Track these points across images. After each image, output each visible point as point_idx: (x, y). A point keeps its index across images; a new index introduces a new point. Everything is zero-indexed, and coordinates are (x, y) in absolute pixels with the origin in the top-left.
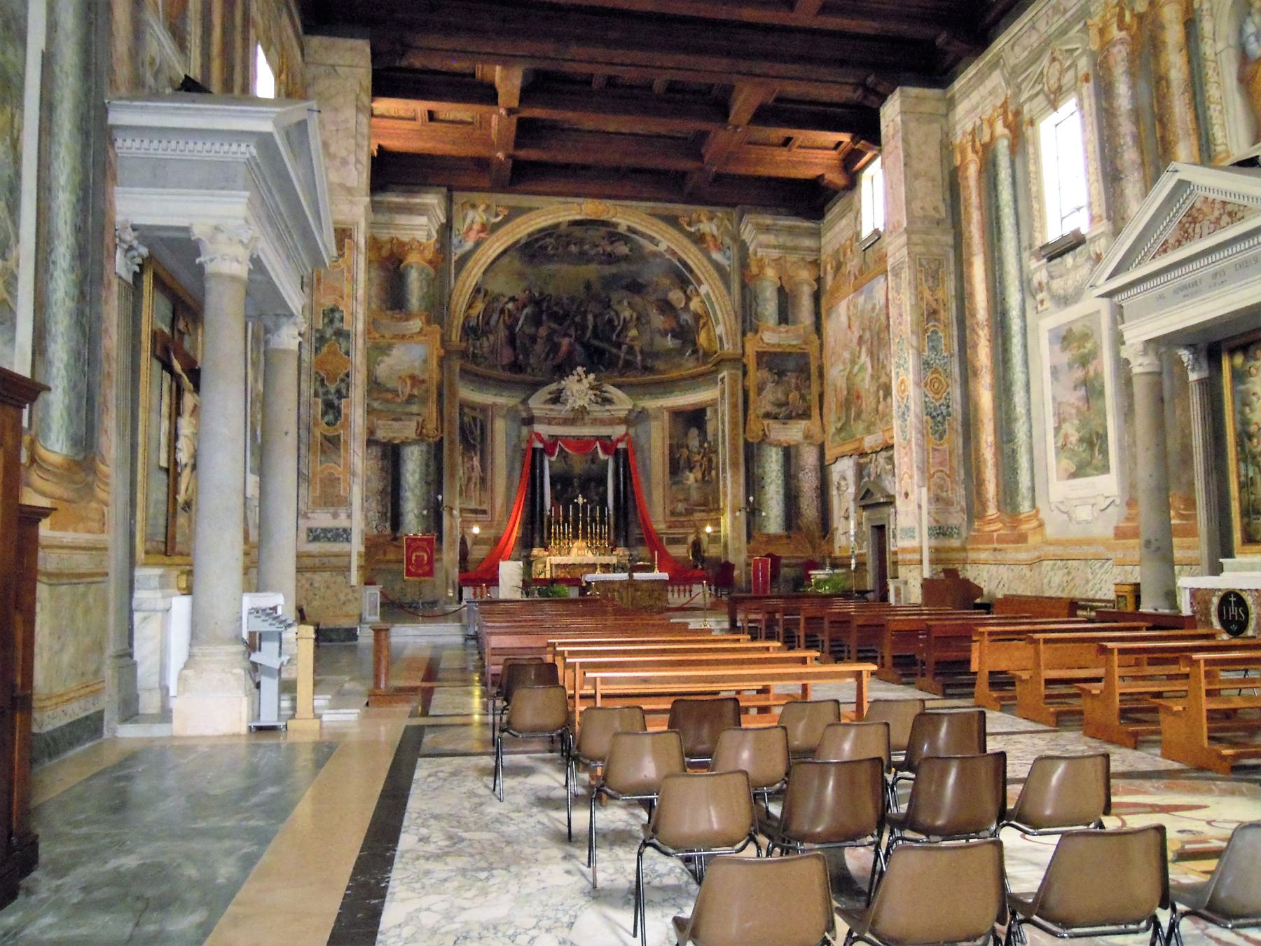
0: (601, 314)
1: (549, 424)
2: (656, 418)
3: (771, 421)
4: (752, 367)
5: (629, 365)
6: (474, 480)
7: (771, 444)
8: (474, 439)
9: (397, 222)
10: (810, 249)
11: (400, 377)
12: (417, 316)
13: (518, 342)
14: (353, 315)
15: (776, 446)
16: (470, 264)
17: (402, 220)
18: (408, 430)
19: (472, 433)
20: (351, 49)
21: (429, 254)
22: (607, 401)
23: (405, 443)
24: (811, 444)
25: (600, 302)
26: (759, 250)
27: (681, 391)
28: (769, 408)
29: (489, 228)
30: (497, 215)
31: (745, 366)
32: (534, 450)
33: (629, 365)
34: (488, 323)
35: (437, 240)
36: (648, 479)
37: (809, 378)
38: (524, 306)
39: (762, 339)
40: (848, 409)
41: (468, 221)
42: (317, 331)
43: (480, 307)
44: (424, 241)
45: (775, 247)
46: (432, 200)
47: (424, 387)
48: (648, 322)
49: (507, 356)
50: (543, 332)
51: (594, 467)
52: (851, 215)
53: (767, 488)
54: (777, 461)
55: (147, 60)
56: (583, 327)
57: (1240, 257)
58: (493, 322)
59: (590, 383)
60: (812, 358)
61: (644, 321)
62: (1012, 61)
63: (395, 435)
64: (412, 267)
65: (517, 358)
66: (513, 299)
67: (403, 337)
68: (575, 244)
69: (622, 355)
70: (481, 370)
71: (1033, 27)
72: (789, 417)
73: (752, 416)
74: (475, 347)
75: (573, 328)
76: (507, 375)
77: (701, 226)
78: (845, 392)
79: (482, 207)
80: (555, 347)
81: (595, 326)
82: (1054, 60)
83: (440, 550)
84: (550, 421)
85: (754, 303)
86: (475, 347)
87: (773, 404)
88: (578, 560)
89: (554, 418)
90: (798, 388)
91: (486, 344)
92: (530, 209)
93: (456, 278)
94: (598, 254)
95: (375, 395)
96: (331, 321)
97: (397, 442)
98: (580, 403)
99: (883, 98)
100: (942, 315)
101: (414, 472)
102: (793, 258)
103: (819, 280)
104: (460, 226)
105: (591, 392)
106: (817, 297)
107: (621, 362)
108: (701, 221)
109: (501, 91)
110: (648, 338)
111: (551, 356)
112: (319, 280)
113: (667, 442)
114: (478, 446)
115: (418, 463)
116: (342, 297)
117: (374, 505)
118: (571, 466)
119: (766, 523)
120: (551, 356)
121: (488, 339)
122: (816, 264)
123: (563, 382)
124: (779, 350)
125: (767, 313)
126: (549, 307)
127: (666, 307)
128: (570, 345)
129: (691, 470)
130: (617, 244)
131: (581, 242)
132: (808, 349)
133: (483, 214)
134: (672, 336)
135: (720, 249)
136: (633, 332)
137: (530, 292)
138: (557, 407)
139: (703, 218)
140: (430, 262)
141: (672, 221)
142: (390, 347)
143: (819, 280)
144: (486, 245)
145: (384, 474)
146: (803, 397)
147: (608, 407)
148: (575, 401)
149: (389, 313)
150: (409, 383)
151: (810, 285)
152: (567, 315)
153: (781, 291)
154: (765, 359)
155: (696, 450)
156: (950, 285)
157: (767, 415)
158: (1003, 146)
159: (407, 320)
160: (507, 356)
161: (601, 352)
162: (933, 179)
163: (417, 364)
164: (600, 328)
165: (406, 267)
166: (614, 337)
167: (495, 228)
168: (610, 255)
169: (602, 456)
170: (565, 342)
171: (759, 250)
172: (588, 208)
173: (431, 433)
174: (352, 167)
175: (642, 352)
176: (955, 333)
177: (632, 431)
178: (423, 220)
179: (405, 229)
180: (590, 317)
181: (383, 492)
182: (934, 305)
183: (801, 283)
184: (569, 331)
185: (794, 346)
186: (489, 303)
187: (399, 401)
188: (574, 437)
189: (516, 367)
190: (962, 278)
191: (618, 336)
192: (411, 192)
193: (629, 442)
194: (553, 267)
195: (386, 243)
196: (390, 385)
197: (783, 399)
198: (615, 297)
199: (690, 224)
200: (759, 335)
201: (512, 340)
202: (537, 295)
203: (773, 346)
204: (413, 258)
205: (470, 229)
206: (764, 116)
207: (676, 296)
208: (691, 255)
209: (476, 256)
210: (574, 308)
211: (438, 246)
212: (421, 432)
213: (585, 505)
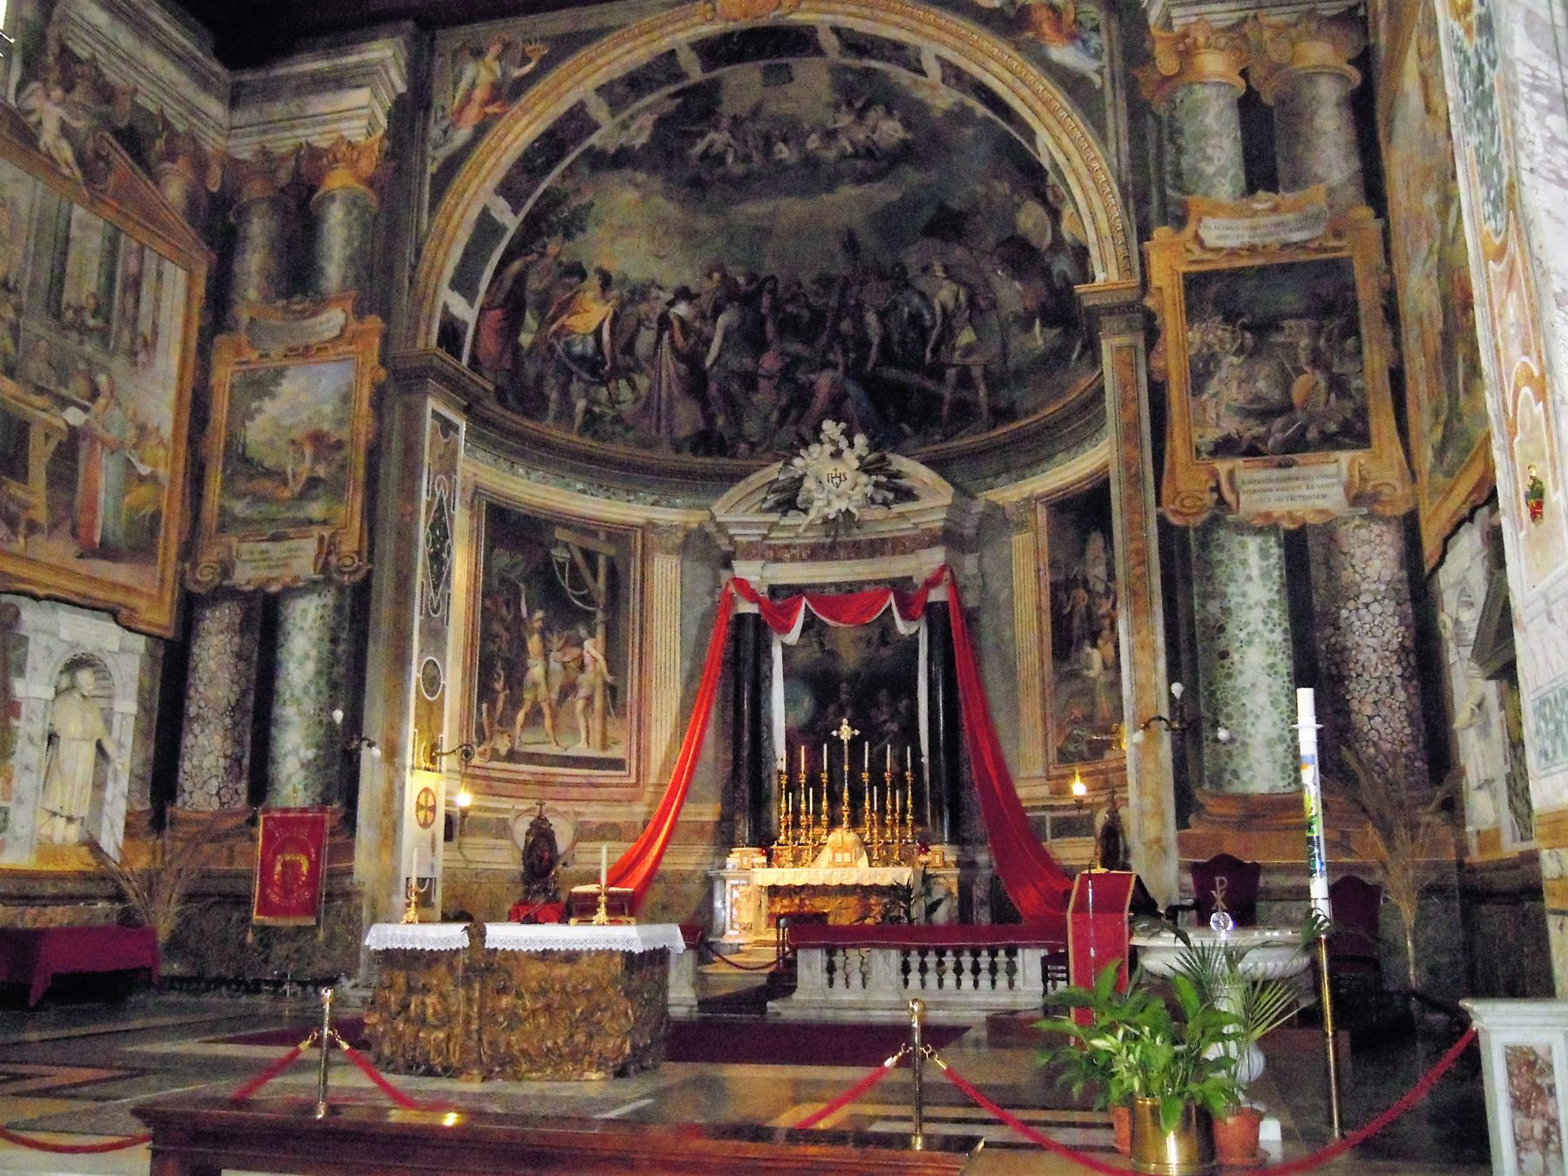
0: (895, 306)
1: (777, 560)
2: (1022, 526)
3: (1240, 462)
4: (1171, 320)
6: (583, 692)
7: (1241, 528)
8: (587, 600)
9: (310, 111)
11: (293, 442)
12: (338, 301)
13: (713, 388)
15: (1259, 531)
17: (322, 104)
18: (302, 558)
19: (577, 582)
21: (367, 166)
22: (906, 495)
23: (291, 591)
24: (1371, 517)
25: (882, 276)
26: (1175, 12)
27: (1068, 449)
28: (1231, 426)
29: (505, 90)
30: (525, 60)
31: (1150, 316)
32: (741, 618)
33: (964, 413)
34: (629, 348)
35: (387, 135)
36: (1011, 673)
37: (1352, 328)
38: (717, 311)
39: (1198, 239)
40: (1450, 366)
41: (463, 85)
47: (338, 456)
48: (994, 305)
49: (687, 417)
50: (770, 362)
51: (886, 652)
53: (1236, 657)
54: (1265, 575)
56: (863, 344)
59: (860, 458)
60: (1359, 272)
61: (983, 304)
63: (275, 573)
64: (333, 199)
65: (710, 419)
66: (684, 294)
68: (785, 140)
69: (947, 394)
70: (618, 449)
72: (1297, 445)
73: (1177, 445)
74: (593, 401)
75: (837, 347)
76: (688, 460)
78: (1440, 325)
79: (495, 50)
80: (802, 397)
81: (886, 341)
83: (348, 850)
84: (776, 555)
85: (1170, 148)
86: (593, 401)
87: (1246, 413)
88: (836, 878)
89: (788, 547)
90: (1317, 360)
91: (625, 392)
92: (601, 32)
93: (433, 206)
94: (843, 157)
95: (241, 485)
97: (274, 588)
98: (842, 505)
101: (307, 656)
104: (446, 99)
105: (864, 478)
107: (945, 409)
110: (998, 340)
111: (794, 413)
113: (1046, 579)
114: (600, 616)
115: (315, 634)
117: (218, 739)
118: (833, 655)
119: (1239, 763)
121: (633, 387)
123: (797, 462)
124: (1259, 261)
125: (1210, 169)
126: (776, 307)
128: (834, 383)
129: (1094, 645)
130: (874, 115)
132: (1345, 248)
133: (496, 66)
135: (1072, 37)
136: (966, 337)
137: (724, 276)
138: (793, 519)
140: (370, 182)
142: (279, 374)
144: (499, 128)
145: (241, 665)
146: (1338, 385)
147: (898, 508)
148: (829, 504)
149: (281, 303)
150: (308, 451)
151: (1341, 77)
153: (1249, 105)
154: (1211, 292)
155: (1100, 588)
157: (1226, 447)
159: (314, 314)
160: (687, 417)
161: (900, 392)
163: (328, 409)
164: (896, 338)
165: (324, 198)
166: (928, 355)
167: (518, 88)
169: (903, 628)
170: (824, 382)
171: (1175, 12)
173: (348, 562)
175: (987, 375)
177: (970, 563)
178: (360, 97)
179: (325, 123)
180: (871, 318)
181: (236, 708)
183: (1311, 77)
184: (831, 357)
185: (1302, 246)
186: (622, 305)
187: (287, 494)
188: (837, 585)
189: (706, 441)
191: (935, 352)
193: (956, 589)
194: (754, 209)
195: (284, 158)
196: (269, 463)
197: (1276, 395)
198: (912, 260)
200: (1189, 231)
201: (696, 382)
202: (741, 280)
203: (1233, 253)
204: (338, 180)
205: (468, 98)
207: (1030, 218)
208: (993, 65)
209: (476, 155)
210: (833, 302)
211: (387, 144)
212: (326, 564)
213: (855, 743)
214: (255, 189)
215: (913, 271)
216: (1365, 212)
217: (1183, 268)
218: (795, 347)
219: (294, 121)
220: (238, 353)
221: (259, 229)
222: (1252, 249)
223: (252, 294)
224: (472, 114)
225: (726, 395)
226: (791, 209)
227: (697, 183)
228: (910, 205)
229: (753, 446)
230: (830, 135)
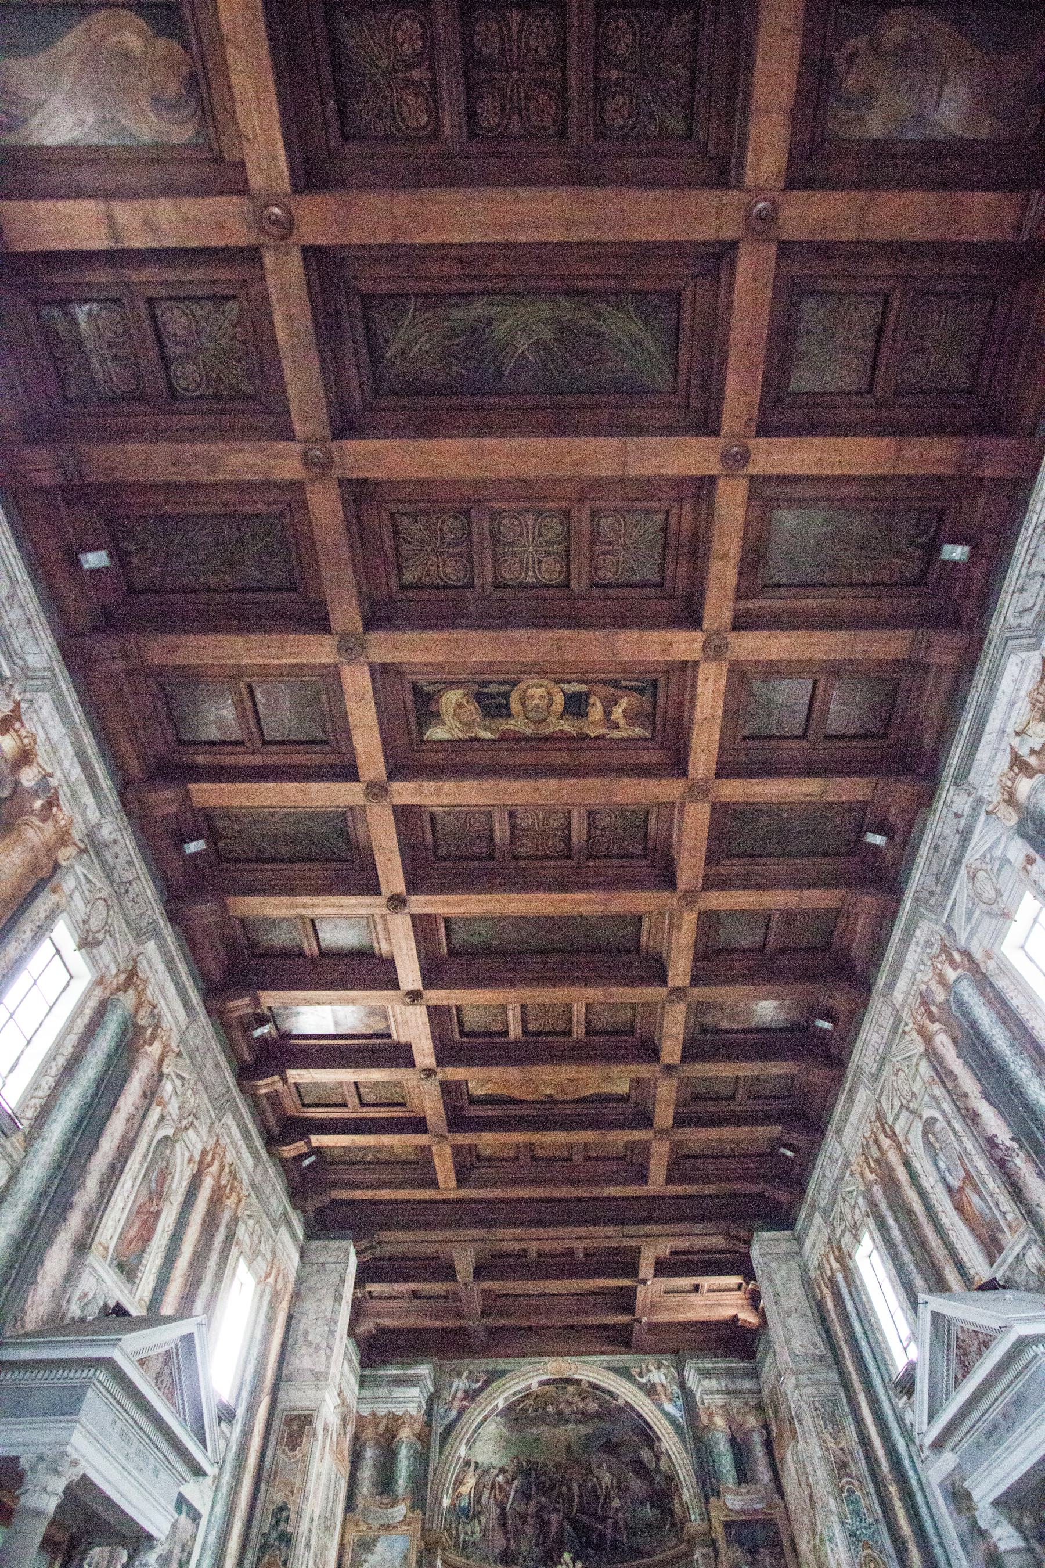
5: (616, 1546)
10: (750, 1392)
13: (509, 1522)
14: (299, 1514)
16: (454, 1434)
17: (400, 1392)
20: (339, 1249)
21: (417, 1428)
34: (479, 1502)
37: (782, 1553)
38: (514, 1478)
42: (264, 1535)
43: (470, 1482)
44: (414, 1413)
45: (718, 1392)
46: (424, 1370)
49: (499, 1541)
50: (532, 1507)
52: (771, 1352)
55: (78, 1293)
57: (1010, 1394)
58: (484, 1501)
62: (823, 1204)
65: (508, 1544)
66: (502, 1471)
67: (386, 1527)
69: (608, 1531)
71: (824, 1176)
74: (466, 1534)
77: (650, 1376)
79: (465, 1374)
81: (581, 1497)
82: (844, 1200)
86: (466, 1534)
92: (505, 1372)
93: (442, 1448)
96: (277, 1523)
99: (748, 1243)
100: (853, 1468)
102: (737, 1403)
103: (766, 1426)
106: (769, 1445)
108: (649, 1371)
109: (459, 1267)
111: (541, 1539)
112: (276, 1472)
116: (292, 1492)
120: (541, 1539)
122: (760, 1407)
124: (744, 1518)
126: (537, 1477)
127: (641, 1469)
128: (560, 1523)
131: (555, 1402)
134: (653, 1506)
136: (616, 1503)
139: (651, 1368)
140: (418, 1436)
141: (624, 1372)
142: (376, 1539)
143: (766, 1426)
152: (552, 1488)
153: (732, 1441)
156: (852, 1429)
158: (840, 1276)
159: (392, 1506)
160: (499, 1541)
162: (804, 1315)
168: (583, 1413)
172: (555, 1366)
174: (322, 1352)
176: (872, 1491)
178: (415, 1391)
180: (575, 1486)
182: (843, 1458)
190: (859, 1421)
191: (603, 1507)
192: (408, 1365)
198: (594, 1460)
199: (641, 1375)
204: (405, 1433)
205: (455, 1397)
206: (663, 1268)
207: (646, 1455)
214: (369, 1433)
215: (594, 1466)
216: (776, 1496)
217: (722, 1518)
218: (544, 1499)
219: (386, 1399)
220: (357, 1525)
221: (370, 1454)
222: (744, 1512)
223: (365, 1491)
224: (456, 1404)
225: (515, 1527)
226: (548, 1432)
227: (516, 1420)
228: (596, 1436)
229: (525, 1558)
230: (569, 1404)
